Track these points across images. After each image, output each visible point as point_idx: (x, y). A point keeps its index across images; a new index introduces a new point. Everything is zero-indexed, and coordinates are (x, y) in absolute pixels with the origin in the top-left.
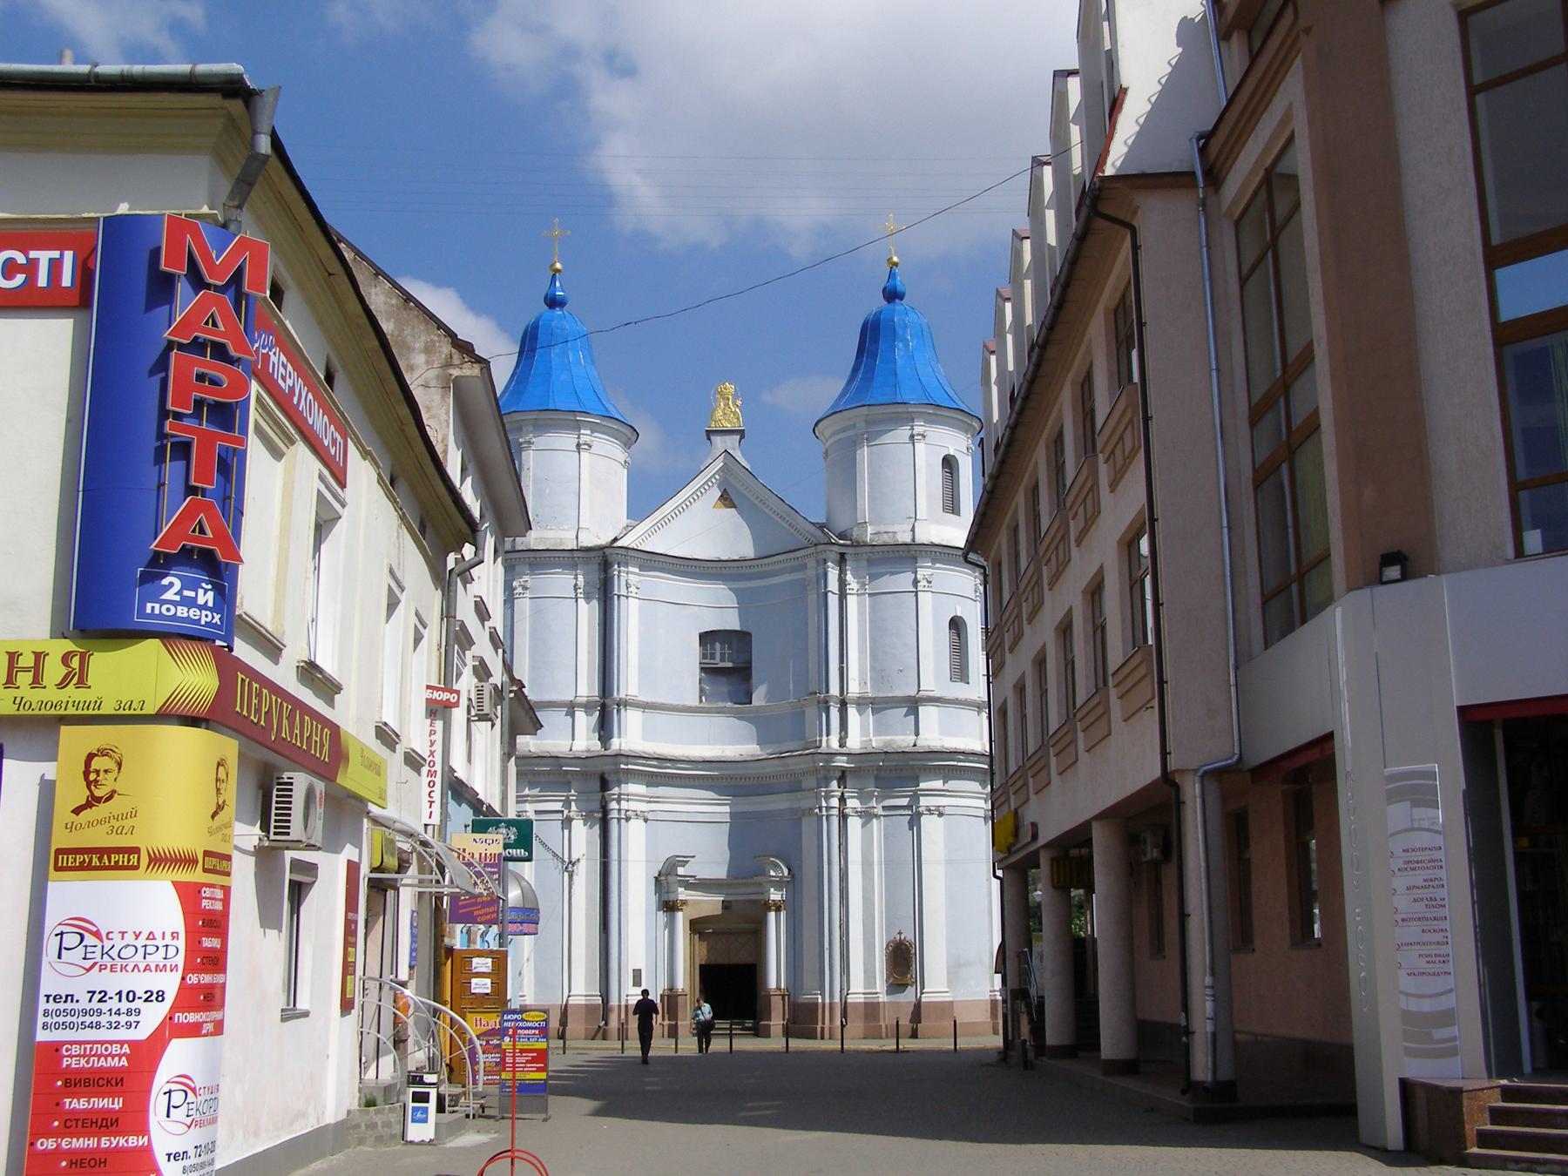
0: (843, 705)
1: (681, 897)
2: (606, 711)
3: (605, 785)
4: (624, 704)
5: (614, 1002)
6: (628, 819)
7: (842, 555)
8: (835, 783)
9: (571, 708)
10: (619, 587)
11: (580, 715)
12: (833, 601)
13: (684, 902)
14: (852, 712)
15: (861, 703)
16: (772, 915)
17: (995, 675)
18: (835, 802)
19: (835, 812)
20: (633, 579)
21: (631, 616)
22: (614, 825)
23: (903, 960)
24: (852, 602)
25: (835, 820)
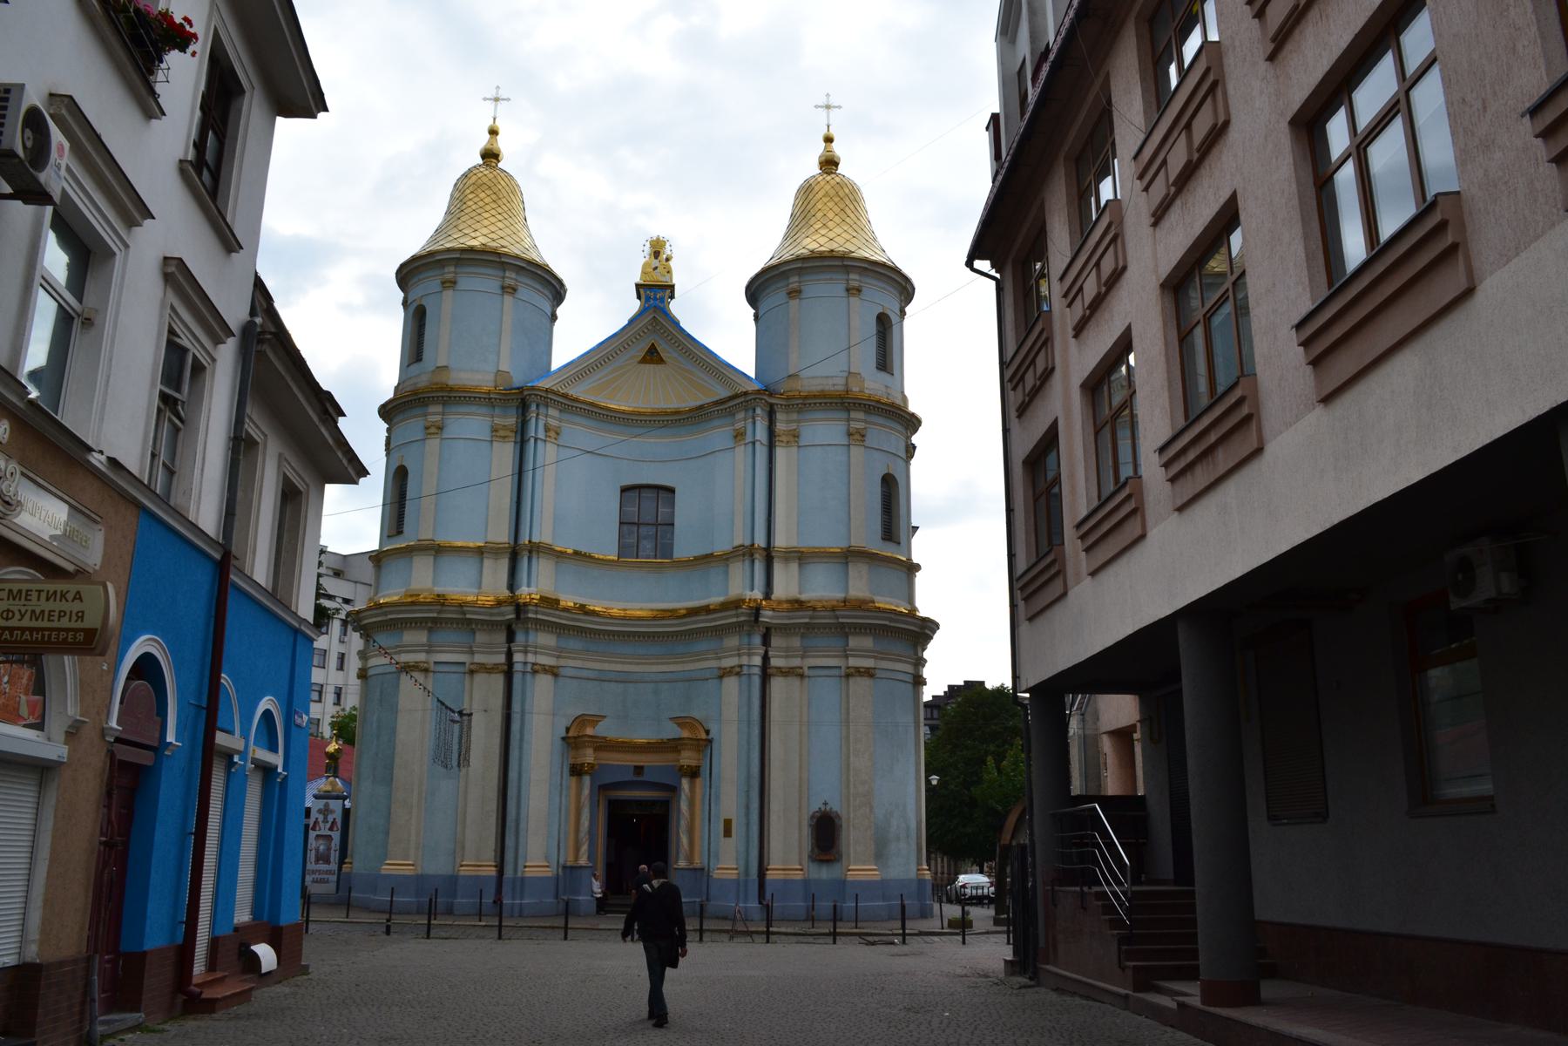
1: (590, 759)
2: (516, 554)
3: (511, 638)
4: (536, 549)
5: (509, 872)
6: (535, 672)
7: (772, 405)
8: (757, 640)
9: (480, 552)
10: (536, 428)
11: (487, 563)
12: (761, 453)
13: (591, 766)
14: (778, 568)
16: (685, 783)
17: (1022, 410)
18: (757, 661)
19: (757, 671)
22: (517, 678)
23: (826, 833)
24: (780, 453)
25: (757, 681)
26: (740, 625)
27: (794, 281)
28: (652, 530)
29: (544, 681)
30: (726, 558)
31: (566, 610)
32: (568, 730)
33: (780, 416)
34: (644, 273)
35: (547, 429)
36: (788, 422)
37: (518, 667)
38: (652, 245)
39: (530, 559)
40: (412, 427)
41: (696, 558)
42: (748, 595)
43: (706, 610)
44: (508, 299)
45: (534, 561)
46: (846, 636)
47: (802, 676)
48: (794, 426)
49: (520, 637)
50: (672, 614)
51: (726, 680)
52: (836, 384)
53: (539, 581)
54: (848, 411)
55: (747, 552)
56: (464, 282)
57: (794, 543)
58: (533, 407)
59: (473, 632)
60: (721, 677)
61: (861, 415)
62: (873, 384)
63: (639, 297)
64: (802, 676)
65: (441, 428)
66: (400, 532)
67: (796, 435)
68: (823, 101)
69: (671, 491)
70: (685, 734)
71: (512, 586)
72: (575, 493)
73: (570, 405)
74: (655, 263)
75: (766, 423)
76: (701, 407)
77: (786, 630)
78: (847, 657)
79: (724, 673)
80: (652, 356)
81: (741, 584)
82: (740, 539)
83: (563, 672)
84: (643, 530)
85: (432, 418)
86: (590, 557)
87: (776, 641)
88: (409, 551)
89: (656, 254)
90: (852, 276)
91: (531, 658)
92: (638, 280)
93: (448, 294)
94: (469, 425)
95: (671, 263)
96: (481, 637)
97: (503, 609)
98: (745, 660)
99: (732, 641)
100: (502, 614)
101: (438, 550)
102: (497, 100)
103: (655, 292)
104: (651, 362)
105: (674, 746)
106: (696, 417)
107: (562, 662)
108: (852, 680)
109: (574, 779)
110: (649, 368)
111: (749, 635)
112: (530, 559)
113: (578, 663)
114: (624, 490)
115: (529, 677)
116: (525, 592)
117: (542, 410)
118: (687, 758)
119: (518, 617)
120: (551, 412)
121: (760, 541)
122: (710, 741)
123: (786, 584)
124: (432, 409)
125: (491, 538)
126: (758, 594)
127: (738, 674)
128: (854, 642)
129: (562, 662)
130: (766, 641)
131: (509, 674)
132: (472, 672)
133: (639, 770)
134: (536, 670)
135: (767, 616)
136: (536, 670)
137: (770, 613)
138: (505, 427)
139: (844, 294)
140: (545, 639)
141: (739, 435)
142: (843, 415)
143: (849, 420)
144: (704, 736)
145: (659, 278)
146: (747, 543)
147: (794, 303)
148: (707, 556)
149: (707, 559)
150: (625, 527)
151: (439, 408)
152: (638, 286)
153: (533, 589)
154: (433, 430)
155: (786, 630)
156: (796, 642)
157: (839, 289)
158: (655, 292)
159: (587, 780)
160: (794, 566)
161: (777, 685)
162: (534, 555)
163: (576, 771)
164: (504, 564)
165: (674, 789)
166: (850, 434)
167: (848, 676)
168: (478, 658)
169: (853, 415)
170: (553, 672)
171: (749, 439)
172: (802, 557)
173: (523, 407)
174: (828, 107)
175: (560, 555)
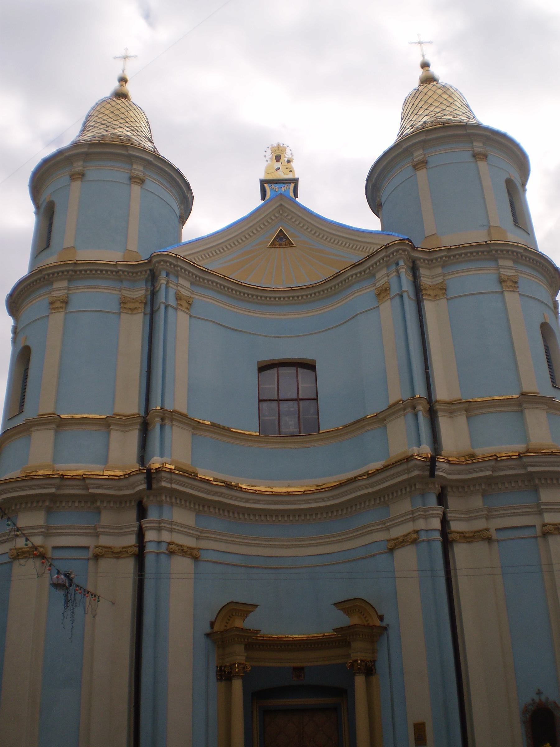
0: (432, 414)
1: (241, 659)
3: (142, 513)
6: (171, 553)
8: (432, 500)
9: (107, 424)
11: (115, 435)
14: (443, 422)
15: (454, 407)
16: (360, 681)
18: (436, 523)
19: (437, 536)
20: (185, 293)
21: (179, 328)
22: (150, 561)
24: (429, 306)
25: (438, 547)
26: (410, 483)
27: (418, 155)
28: (293, 406)
29: (181, 565)
30: (381, 419)
31: (207, 482)
32: (212, 624)
33: (422, 271)
34: (267, 173)
35: (178, 298)
36: (432, 277)
37: (150, 548)
38: (272, 151)
39: (162, 427)
40: (37, 306)
41: (345, 427)
42: (415, 450)
43: (369, 475)
44: (136, 188)
45: (167, 428)
46: (536, 489)
47: (489, 540)
48: (439, 280)
49: (153, 515)
50: (321, 490)
51: (398, 553)
52: (478, 236)
53: (174, 451)
54: (496, 260)
55: (411, 405)
56: (91, 174)
57: (456, 395)
58: (163, 274)
59: (98, 511)
60: (391, 550)
61: (510, 263)
62: (514, 236)
63: (263, 196)
64: (489, 540)
65: (66, 302)
66: (21, 411)
67: (443, 288)
68: (417, 40)
69: (310, 366)
70: (355, 620)
71: (142, 459)
72: (207, 362)
73: (201, 277)
74: (278, 165)
75: (411, 279)
76: (337, 275)
77: (464, 487)
78: (540, 513)
79: (394, 546)
80: (282, 240)
81: (403, 439)
82: (397, 393)
83: (204, 556)
84: (284, 406)
85: (56, 294)
86: (229, 430)
87: (453, 502)
88: (27, 428)
89: (278, 158)
90: (475, 144)
91: (166, 536)
92: (263, 177)
93: (76, 185)
94: (94, 298)
95: (293, 164)
96: (107, 518)
97: (132, 479)
98: (421, 524)
99: (404, 506)
100: (132, 486)
101: (59, 424)
102: (125, 58)
103: (279, 190)
104: (282, 246)
105: (343, 638)
106: (334, 285)
107: (203, 544)
108: (551, 540)
109: (223, 684)
110: (279, 252)
111: (423, 495)
112: (162, 427)
113: (222, 547)
114: (263, 368)
115: (163, 558)
116: (155, 462)
117: (172, 278)
118: (358, 652)
119: (149, 487)
120: (181, 281)
121: (420, 392)
122: (385, 629)
123: (455, 436)
124: (56, 285)
125: (117, 410)
126: (426, 449)
127: (415, 542)
128: (546, 495)
129: (203, 544)
130: (442, 499)
131: (140, 557)
132: (97, 557)
133: (298, 670)
134: (174, 550)
135: (442, 470)
136: (174, 550)
137: (446, 466)
138: (134, 300)
139: (472, 160)
140: (182, 516)
141: (383, 293)
142: (492, 264)
143: (498, 268)
144: (378, 623)
145: (282, 175)
146: (407, 396)
147: (422, 174)
148: (358, 421)
149: (359, 424)
150: (265, 405)
151: (65, 284)
152: (263, 183)
153: (165, 459)
154: (58, 304)
155: (464, 487)
156: (477, 502)
157: (466, 156)
158: (279, 190)
159: (237, 685)
160: (461, 420)
161: (460, 551)
162: (167, 422)
163: (225, 675)
164: (134, 436)
165: (344, 693)
166: (501, 281)
167: (545, 535)
168: (104, 541)
169: (501, 262)
170: (194, 555)
171: (394, 290)
172: (469, 408)
173: (153, 277)
174: (420, 43)
175: (196, 426)
